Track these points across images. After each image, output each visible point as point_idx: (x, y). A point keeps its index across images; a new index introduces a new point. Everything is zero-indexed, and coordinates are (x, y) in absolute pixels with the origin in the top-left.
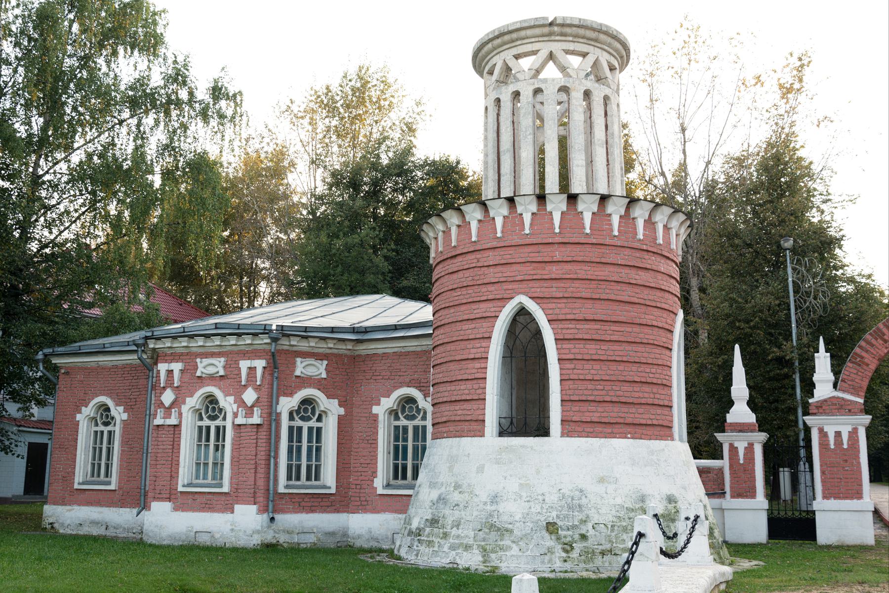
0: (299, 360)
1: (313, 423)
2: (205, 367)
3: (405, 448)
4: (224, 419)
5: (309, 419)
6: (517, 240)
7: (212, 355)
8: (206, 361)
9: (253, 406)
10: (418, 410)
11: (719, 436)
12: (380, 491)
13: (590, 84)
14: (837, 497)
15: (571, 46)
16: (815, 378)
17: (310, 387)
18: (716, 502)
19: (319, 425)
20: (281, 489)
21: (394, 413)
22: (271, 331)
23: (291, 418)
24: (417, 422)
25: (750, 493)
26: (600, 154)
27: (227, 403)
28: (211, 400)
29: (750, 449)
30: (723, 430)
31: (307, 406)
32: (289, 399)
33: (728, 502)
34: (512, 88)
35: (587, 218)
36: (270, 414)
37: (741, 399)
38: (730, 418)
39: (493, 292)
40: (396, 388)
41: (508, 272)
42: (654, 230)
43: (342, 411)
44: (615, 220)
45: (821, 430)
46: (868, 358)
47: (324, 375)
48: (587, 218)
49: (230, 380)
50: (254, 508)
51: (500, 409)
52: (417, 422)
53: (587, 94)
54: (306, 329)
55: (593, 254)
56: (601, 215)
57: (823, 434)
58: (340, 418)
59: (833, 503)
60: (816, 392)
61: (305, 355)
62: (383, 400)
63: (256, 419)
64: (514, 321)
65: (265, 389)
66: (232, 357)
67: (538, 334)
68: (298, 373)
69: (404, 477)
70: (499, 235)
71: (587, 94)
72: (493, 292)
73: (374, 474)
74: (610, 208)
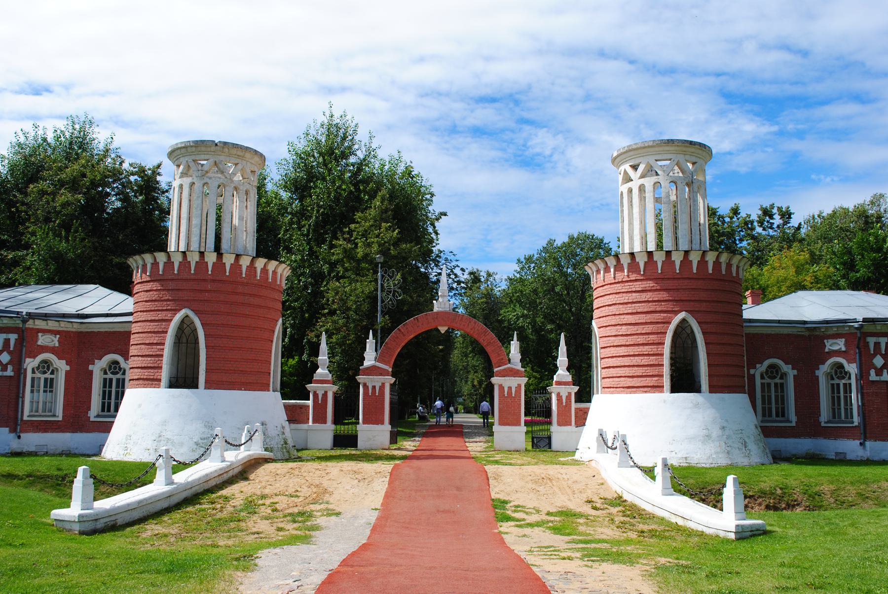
0: (40, 334)
1: (48, 375)
3: (110, 392)
5: (45, 373)
9: (7, 364)
10: (120, 369)
11: (309, 386)
12: (92, 419)
19: (52, 376)
20: (25, 418)
23: (33, 372)
24: (119, 376)
31: (46, 365)
32: (32, 360)
38: (316, 377)
45: (365, 385)
47: (57, 345)
50: (7, 429)
51: (171, 372)
52: (119, 376)
58: (67, 372)
61: (45, 331)
63: (9, 372)
64: (182, 321)
67: (195, 331)
68: (39, 343)
69: (109, 410)
70: (176, 272)
73: (89, 408)
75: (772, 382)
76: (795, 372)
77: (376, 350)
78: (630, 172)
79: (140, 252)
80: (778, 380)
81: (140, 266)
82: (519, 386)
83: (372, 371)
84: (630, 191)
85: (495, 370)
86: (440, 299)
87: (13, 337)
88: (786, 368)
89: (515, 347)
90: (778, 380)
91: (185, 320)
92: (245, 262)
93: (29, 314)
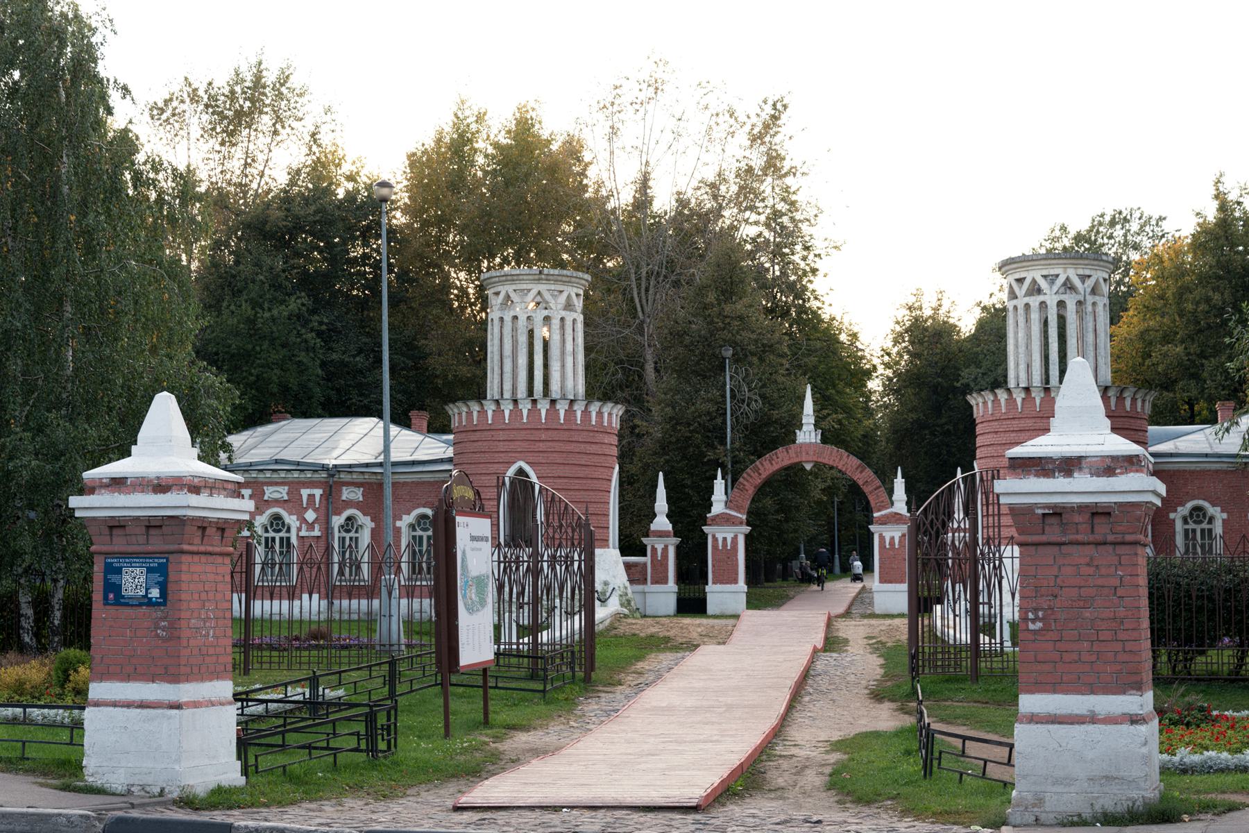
1: (352, 534)
2: (270, 493)
4: (288, 530)
5: (348, 531)
6: (517, 425)
7: (277, 484)
8: (271, 489)
11: (645, 540)
13: (563, 313)
14: (722, 583)
15: (553, 287)
16: (713, 498)
17: (351, 507)
18: (640, 588)
21: (412, 527)
22: (328, 469)
25: (664, 581)
26: (569, 360)
27: (291, 520)
28: (277, 518)
29: (665, 549)
30: (647, 536)
33: (650, 587)
34: (512, 313)
35: (562, 413)
36: (327, 529)
37: (661, 513)
38: (653, 527)
39: (503, 457)
40: (414, 508)
41: (512, 446)
42: (602, 417)
43: (373, 525)
44: (579, 414)
45: (714, 536)
46: (748, 485)
48: (562, 413)
49: (293, 503)
53: (562, 319)
54: (350, 466)
55: (565, 436)
56: (570, 412)
57: (715, 539)
58: (373, 530)
59: (719, 587)
60: (713, 509)
61: (348, 484)
62: (404, 517)
63: (317, 532)
65: (323, 511)
66: (295, 487)
68: (344, 498)
71: (562, 319)
72: (503, 457)
74: (576, 407)
75: (1198, 528)
76: (1225, 516)
77: (726, 493)
78: (1015, 285)
79: (464, 399)
80: (1205, 526)
81: (459, 413)
82: (904, 535)
83: (724, 520)
84: (1015, 308)
85: (875, 515)
86: (805, 428)
87: (318, 492)
88: (1212, 510)
89: (899, 484)
90: (1205, 526)
91: (521, 472)
92: (579, 408)
93: (335, 466)
